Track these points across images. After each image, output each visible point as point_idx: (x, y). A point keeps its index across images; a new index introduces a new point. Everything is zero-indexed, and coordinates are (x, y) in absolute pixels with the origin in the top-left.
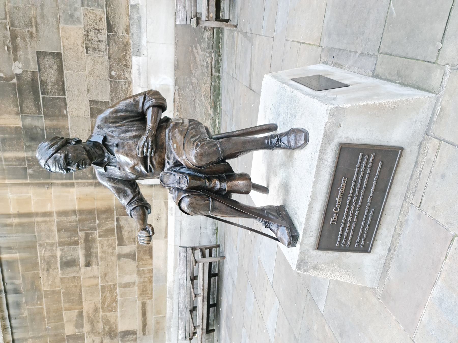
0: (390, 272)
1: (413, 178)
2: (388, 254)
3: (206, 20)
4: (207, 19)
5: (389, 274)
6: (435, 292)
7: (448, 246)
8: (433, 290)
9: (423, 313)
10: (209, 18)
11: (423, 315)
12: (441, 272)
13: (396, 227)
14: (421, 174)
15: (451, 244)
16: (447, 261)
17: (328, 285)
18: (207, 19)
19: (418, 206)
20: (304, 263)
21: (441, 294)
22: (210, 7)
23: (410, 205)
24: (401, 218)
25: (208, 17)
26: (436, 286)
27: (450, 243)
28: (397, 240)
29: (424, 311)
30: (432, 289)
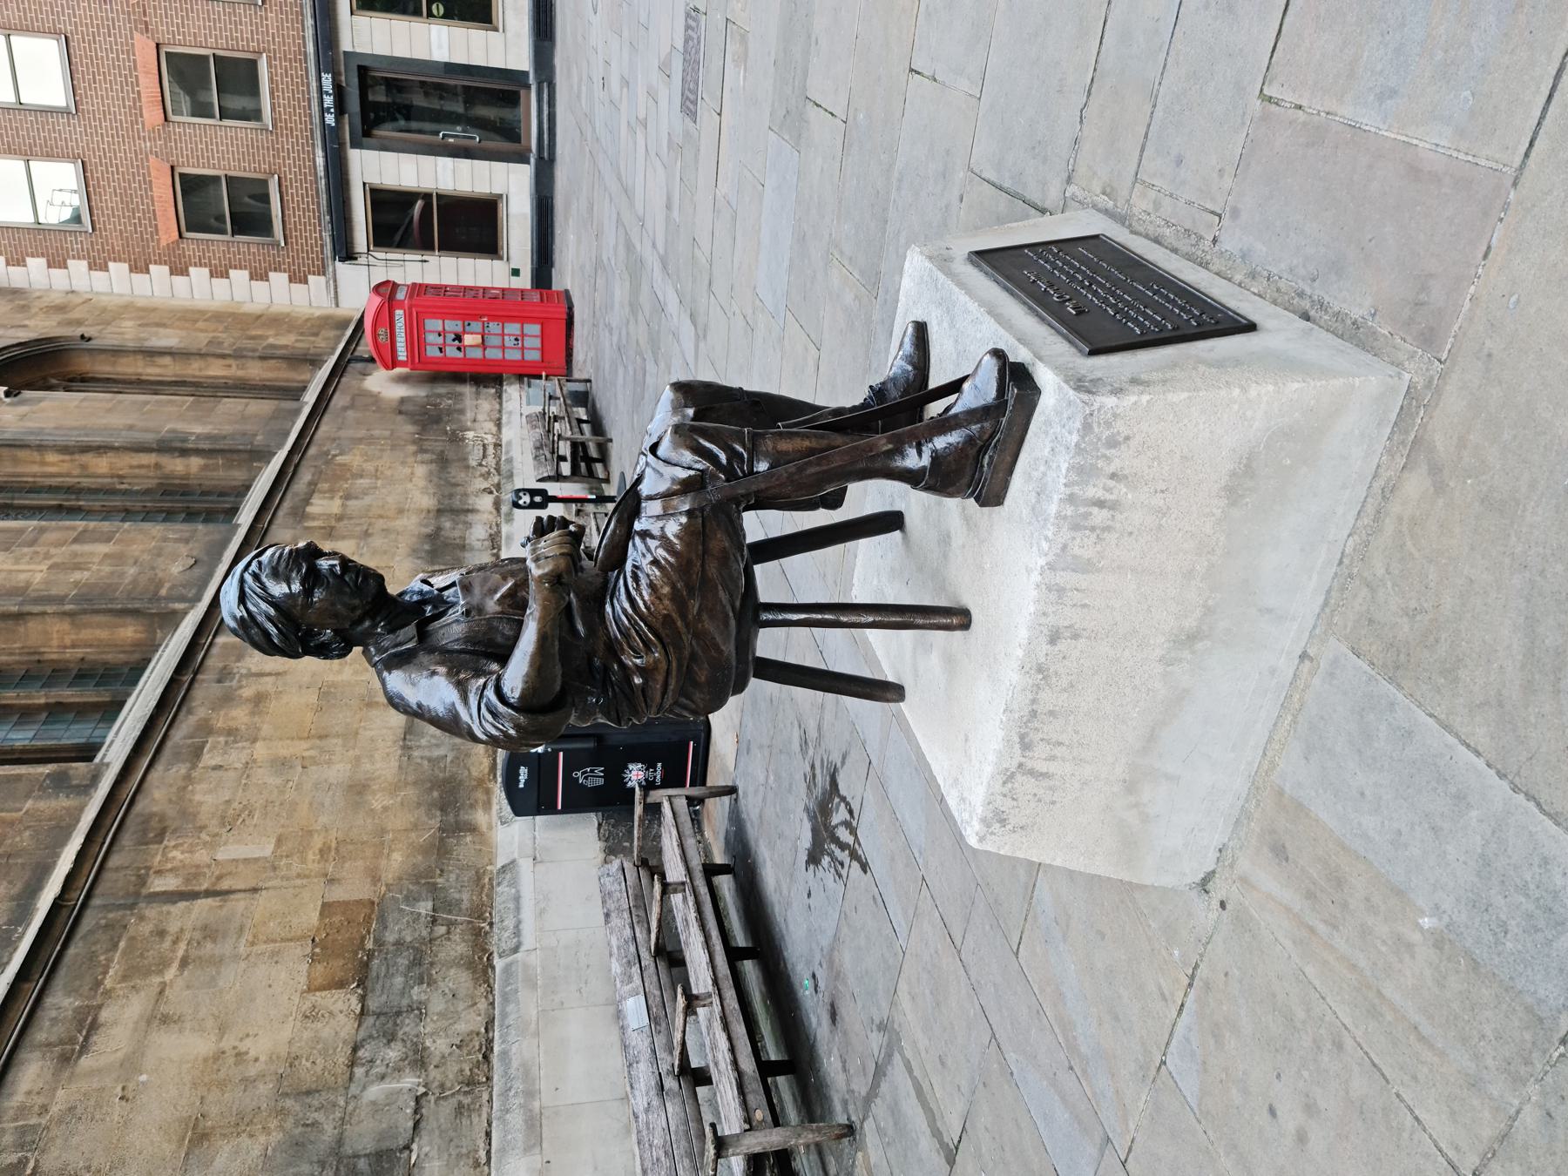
0: (1356, 313)
1: (1176, 244)
2: (1314, 322)
3: (746, 1131)
4: (747, 1127)
5: (1361, 313)
6: (1369, 119)
7: (1278, 108)
8: (1367, 128)
9: (1427, 146)
10: (754, 1124)
11: (1434, 147)
12: (1328, 113)
13: (1255, 294)
14: (1173, 221)
15: (1277, 104)
16: (1304, 103)
17: (1480, 763)
18: (747, 1127)
19: (1217, 218)
20: (1091, 381)
21: (1372, 98)
22: (751, 1098)
23: (1217, 247)
24: (1238, 277)
25: (748, 1120)
26: (1356, 119)
27: (1274, 106)
28: (1282, 284)
29: (1421, 144)
30: (1365, 131)
